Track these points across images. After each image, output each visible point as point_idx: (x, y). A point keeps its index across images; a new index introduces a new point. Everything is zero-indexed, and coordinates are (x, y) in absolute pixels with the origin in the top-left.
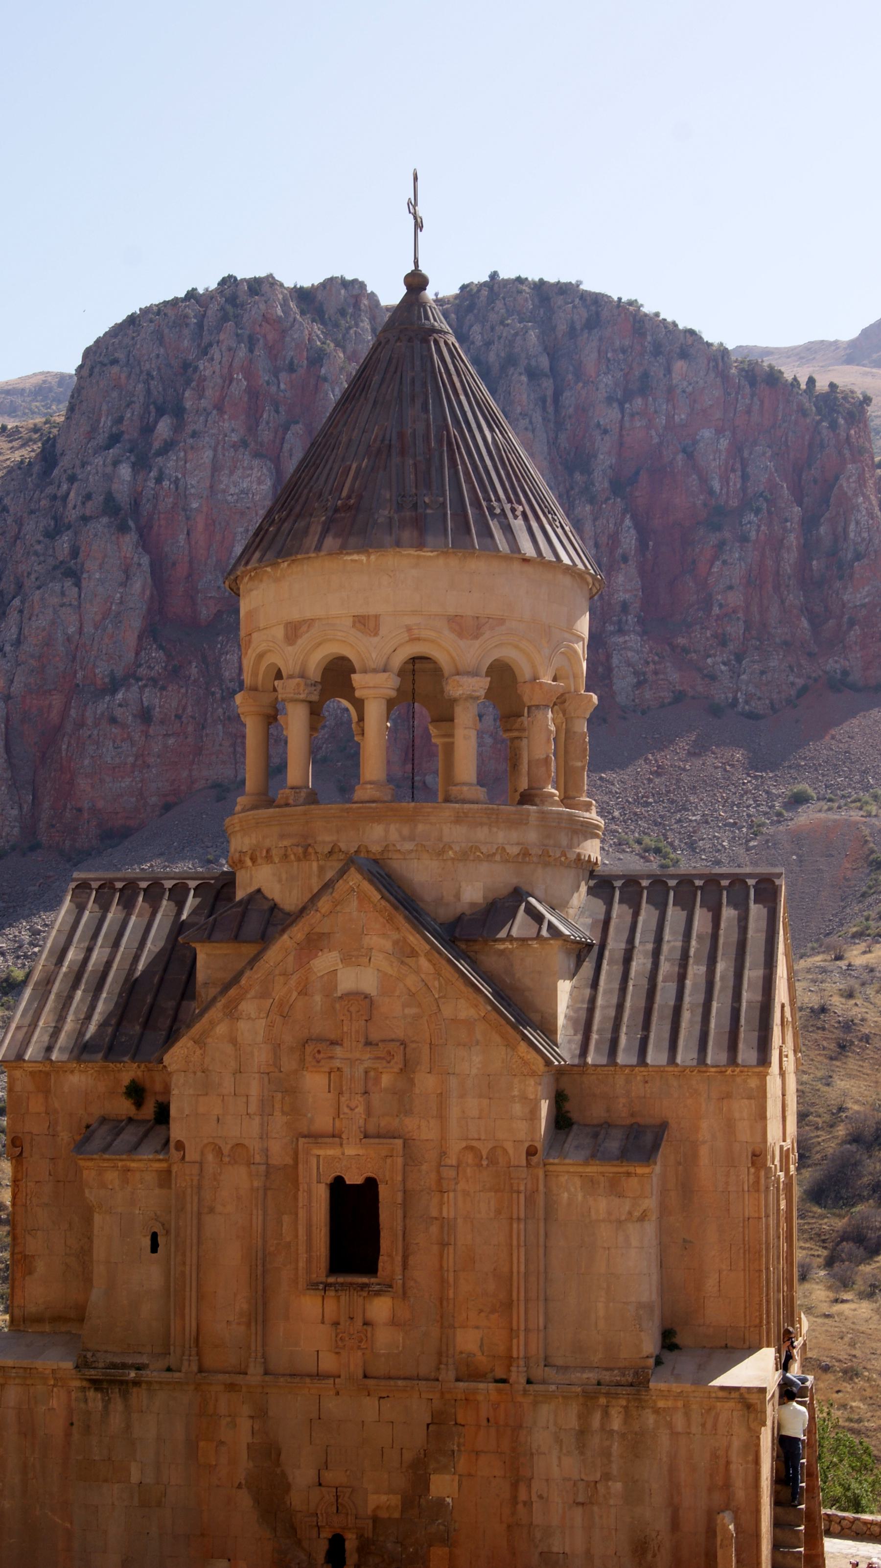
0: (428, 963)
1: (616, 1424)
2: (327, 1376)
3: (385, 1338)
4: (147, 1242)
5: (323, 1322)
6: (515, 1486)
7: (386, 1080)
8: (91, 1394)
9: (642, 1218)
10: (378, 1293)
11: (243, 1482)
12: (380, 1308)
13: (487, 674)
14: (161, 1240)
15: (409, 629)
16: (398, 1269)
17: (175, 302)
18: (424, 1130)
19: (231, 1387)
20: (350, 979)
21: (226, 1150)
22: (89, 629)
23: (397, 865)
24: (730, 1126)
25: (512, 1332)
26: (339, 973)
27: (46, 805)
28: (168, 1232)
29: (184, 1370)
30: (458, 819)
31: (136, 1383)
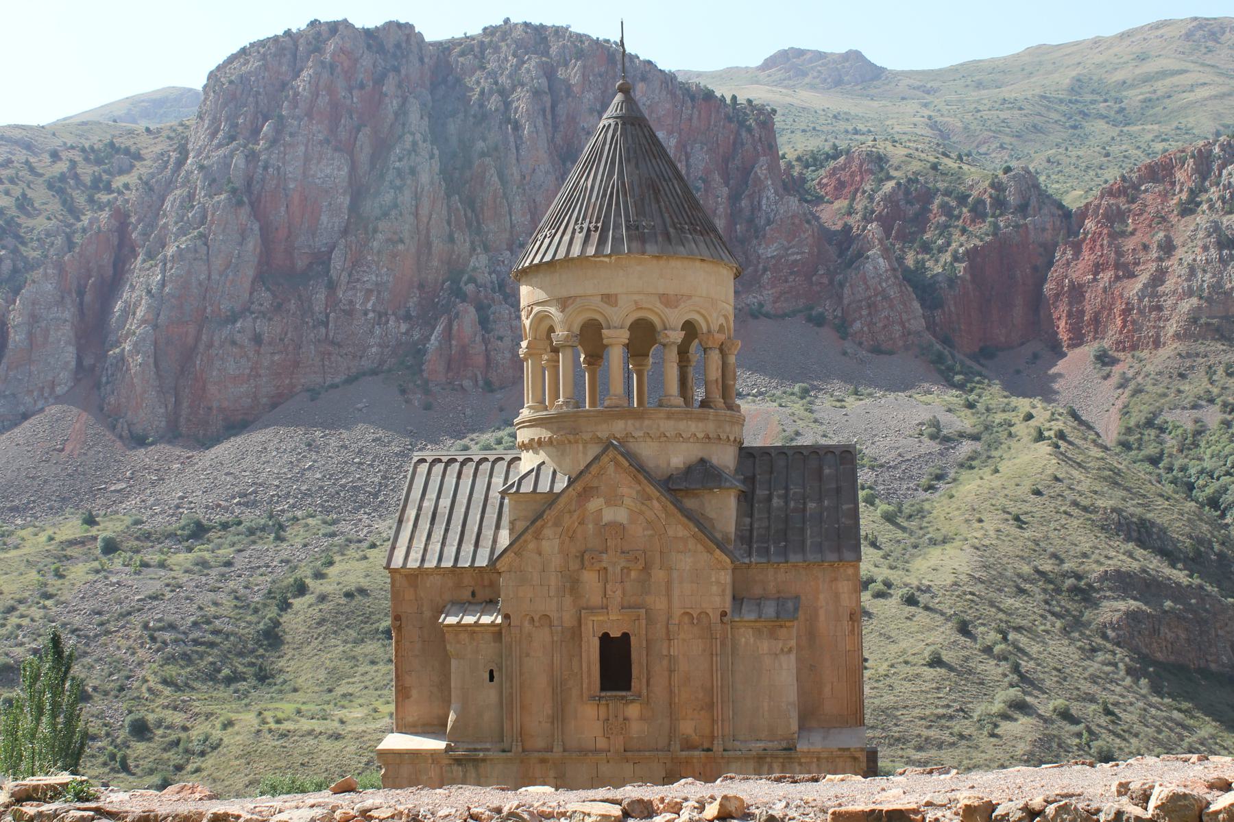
0: (658, 506)
2: (602, 751)
3: (636, 728)
4: (487, 676)
7: (633, 574)
8: (455, 768)
9: (790, 650)
10: (632, 701)
12: (633, 711)
13: (682, 329)
15: (636, 302)
16: (644, 686)
17: (276, 39)
18: (658, 603)
19: (543, 761)
20: (609, 515)
22: (215, 276)
23: (633, 446)
24: (837, 596)
25: (713, 721)
27: (185, 405)
28: (500, 669)
29: (514, 749)
30: (668, 418)
31: (484, 760)
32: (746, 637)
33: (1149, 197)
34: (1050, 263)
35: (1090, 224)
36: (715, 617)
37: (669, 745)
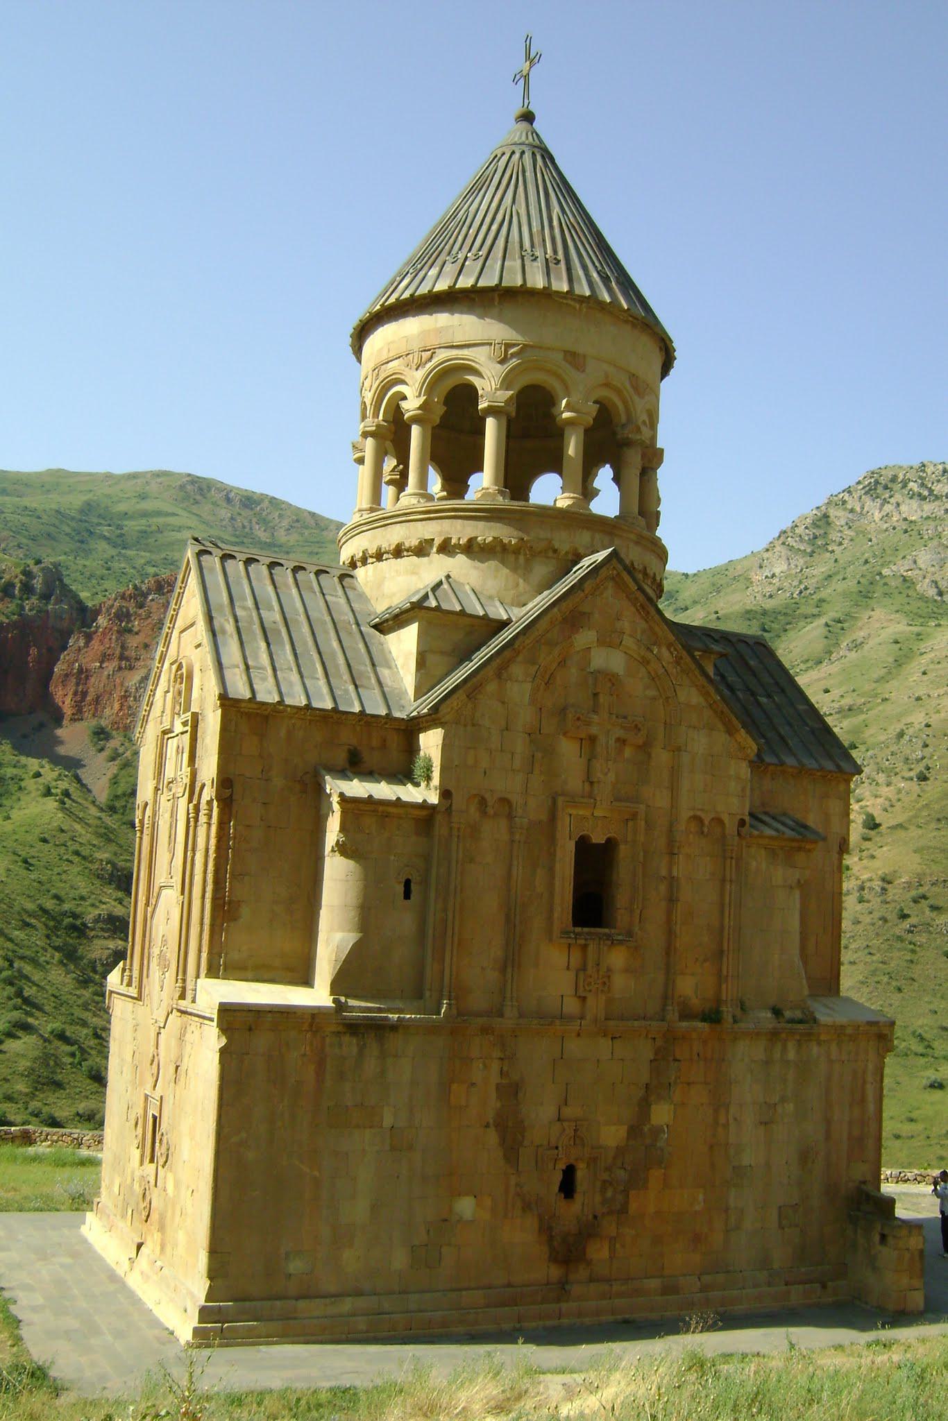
1: (791, 1055)
2: (571, 1018)
3: (620, 982)
4: (400, 889)
5: (568, 968)
6: (716, 1111)
8: (346, 1039)
10: (621, 942)
11: (491, 1121)
12: (617, 958)
14: (413, 887)
15: (607, 376)
18: (661, 800)
19: (485, 1030)
20: (601, 659)
21: (490, 801)
25: (720, 978)
26: (593, 652)
28: (425, 882)
32: (758, 861)
33: (154, 606)
34: (65, 648)
35: (102, 621)
36: (731, 826)
37: (663, 1010)
